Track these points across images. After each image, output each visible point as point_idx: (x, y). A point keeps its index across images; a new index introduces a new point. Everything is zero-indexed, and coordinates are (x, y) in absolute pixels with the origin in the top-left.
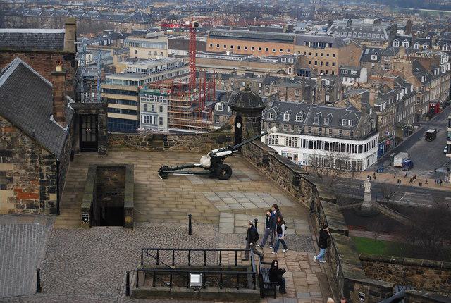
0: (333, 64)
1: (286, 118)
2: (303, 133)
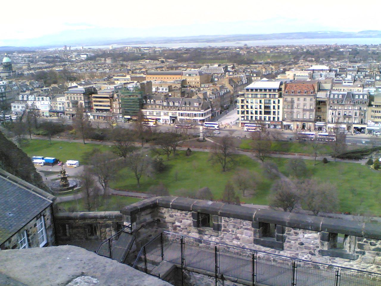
0: (198, 83)
1: (171, 104)
2: (179, 110)
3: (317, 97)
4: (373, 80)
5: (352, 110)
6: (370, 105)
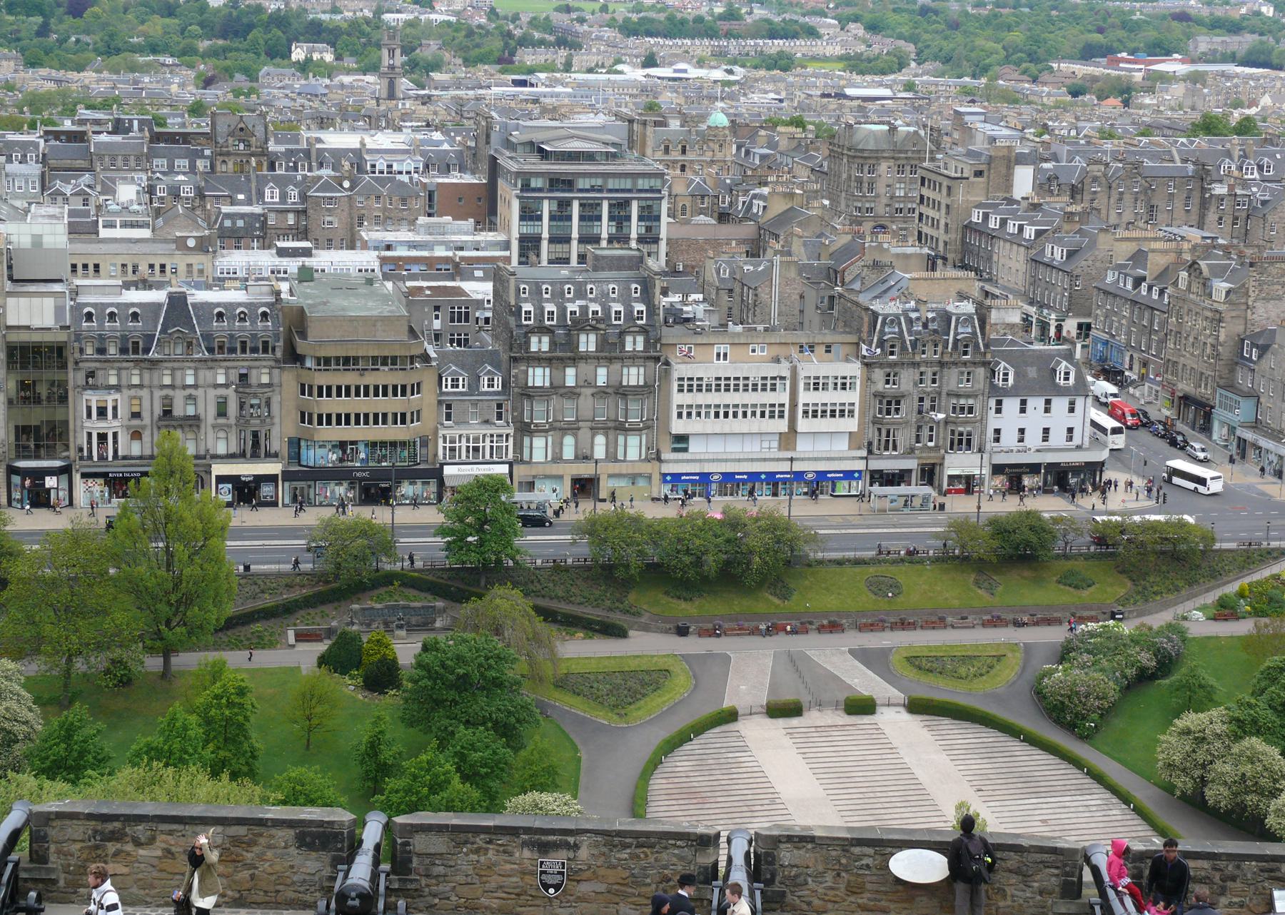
3: (11, 321)
4: (257, 209)
5: (204, 387)
6: (294, 357)
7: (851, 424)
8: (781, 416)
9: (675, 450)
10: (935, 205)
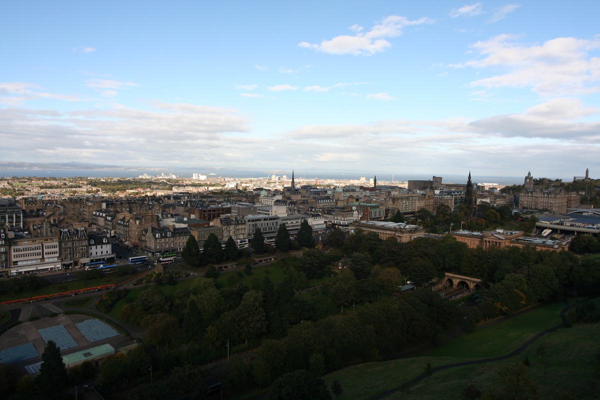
7: (58, 255)
8: (40, 255)
9: (14, 265)
10: (86, 212)
